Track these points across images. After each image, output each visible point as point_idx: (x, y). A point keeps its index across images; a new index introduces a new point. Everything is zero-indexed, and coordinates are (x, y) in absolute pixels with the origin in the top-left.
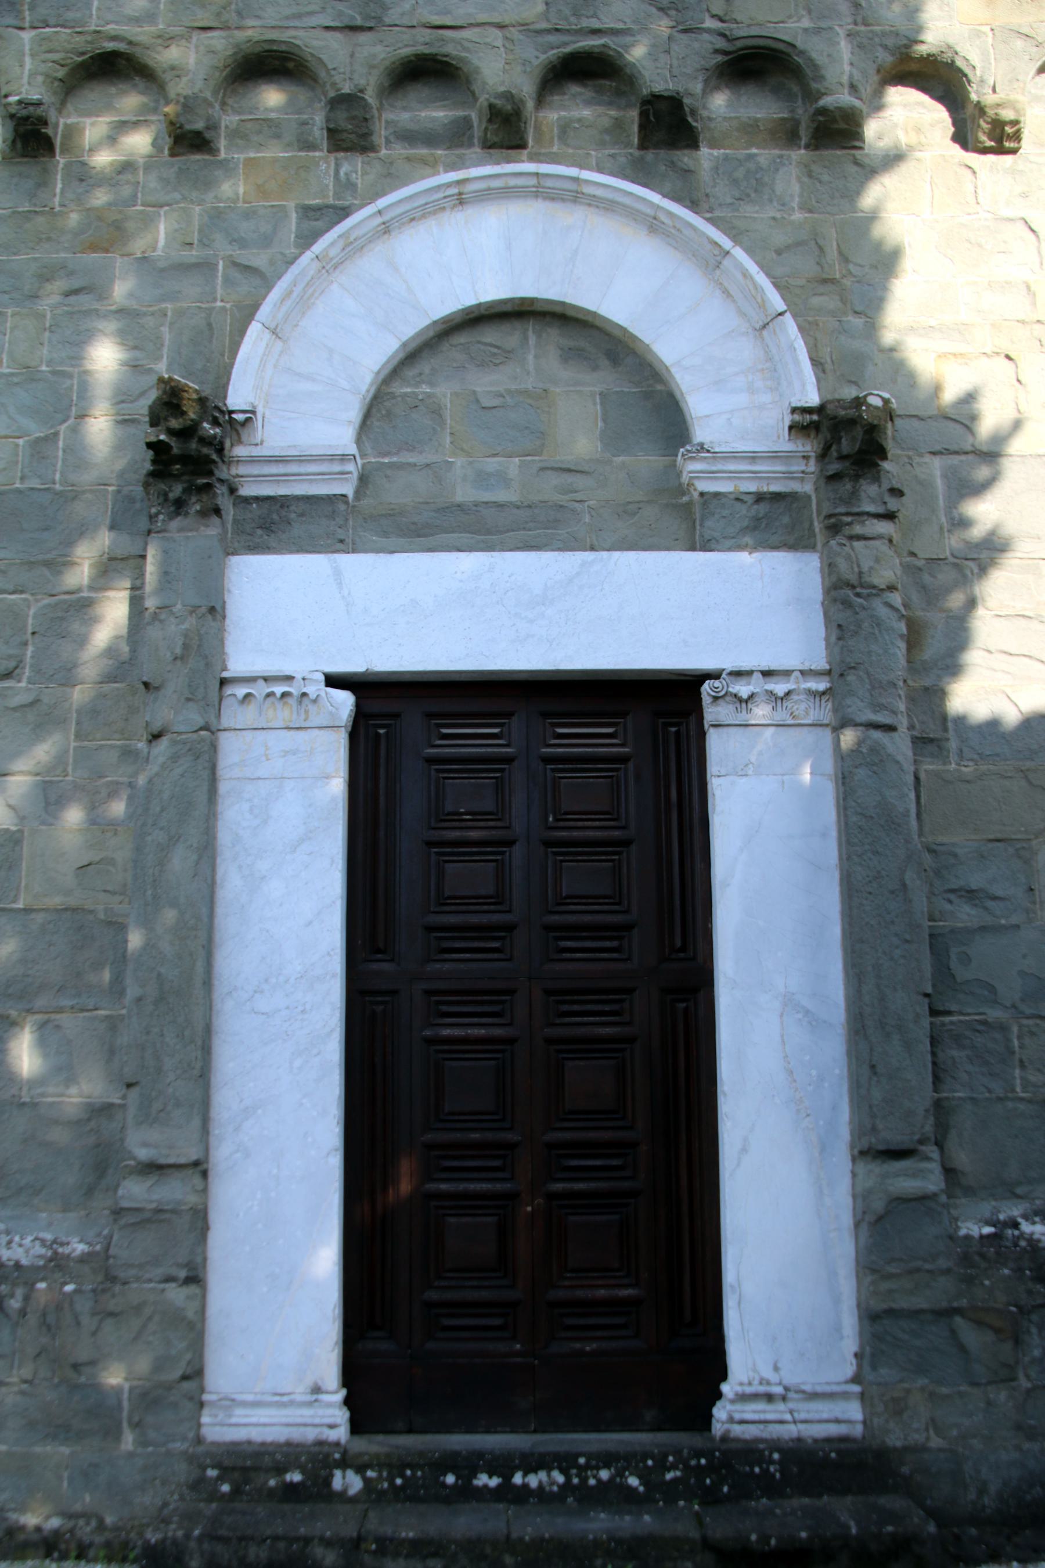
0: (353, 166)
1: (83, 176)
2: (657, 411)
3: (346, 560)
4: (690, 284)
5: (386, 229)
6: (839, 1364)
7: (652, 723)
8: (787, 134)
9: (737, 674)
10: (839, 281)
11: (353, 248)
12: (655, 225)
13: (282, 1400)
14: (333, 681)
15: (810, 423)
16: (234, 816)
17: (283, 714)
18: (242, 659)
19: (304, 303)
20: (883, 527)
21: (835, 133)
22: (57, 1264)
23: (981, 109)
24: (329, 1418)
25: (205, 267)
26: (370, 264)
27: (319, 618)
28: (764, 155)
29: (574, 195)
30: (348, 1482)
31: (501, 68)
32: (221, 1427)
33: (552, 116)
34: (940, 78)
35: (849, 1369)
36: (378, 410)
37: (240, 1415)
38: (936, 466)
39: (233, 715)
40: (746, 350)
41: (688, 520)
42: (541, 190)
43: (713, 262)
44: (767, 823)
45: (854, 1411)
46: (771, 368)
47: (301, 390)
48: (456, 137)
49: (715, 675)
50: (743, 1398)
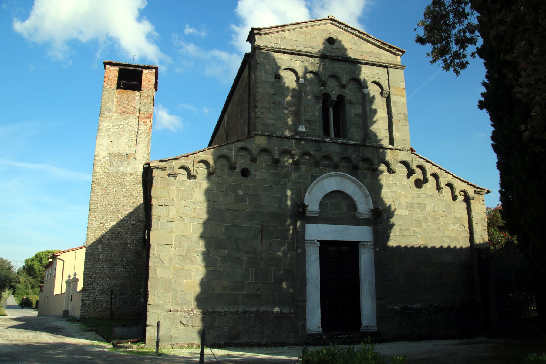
0: (317, 170)
1: (283, 167)
2: (353, 206)
3: (318, 225)
4: (358, 190)
5: (322, 180)
6: (374, 323)
7: (352, 248)
8: (368, 169)
9: (364, 242)
10: (375, 189)
11: (318, 182)
12: (354, 181)
13: (315, 329)
14: (318, 241)
15: (372, 211)
16: (307, 257)
17: (312, 245)
18: (307, 238)
19: (312, 189)
20: (380, 225)
21: (376, 172)
22: (290, 313)
23: (391, 169)
24: (320, 330)
25: (299, 182)
26: (320, 184)
27: (316, 232)
28: (366, 172)
29: (344, 176)
30: (324, 337)
31: (336, 158)
32: (309, 332)
33: (341, 164)
34: (387, 164)
35: (375, 324)
36: (322, 205)
37: (311, 330)
38: (385, 215)
39: (307, 245)
40: (364, 199)
41: (358, 222)
42: (341, 176)
43: (361, 187)
44: (366, 260)
45: (376, 328)
46: (367, 202)
47: (313, 201)
48: (329, 166)
49: (361, 242)
50: (365, 327)
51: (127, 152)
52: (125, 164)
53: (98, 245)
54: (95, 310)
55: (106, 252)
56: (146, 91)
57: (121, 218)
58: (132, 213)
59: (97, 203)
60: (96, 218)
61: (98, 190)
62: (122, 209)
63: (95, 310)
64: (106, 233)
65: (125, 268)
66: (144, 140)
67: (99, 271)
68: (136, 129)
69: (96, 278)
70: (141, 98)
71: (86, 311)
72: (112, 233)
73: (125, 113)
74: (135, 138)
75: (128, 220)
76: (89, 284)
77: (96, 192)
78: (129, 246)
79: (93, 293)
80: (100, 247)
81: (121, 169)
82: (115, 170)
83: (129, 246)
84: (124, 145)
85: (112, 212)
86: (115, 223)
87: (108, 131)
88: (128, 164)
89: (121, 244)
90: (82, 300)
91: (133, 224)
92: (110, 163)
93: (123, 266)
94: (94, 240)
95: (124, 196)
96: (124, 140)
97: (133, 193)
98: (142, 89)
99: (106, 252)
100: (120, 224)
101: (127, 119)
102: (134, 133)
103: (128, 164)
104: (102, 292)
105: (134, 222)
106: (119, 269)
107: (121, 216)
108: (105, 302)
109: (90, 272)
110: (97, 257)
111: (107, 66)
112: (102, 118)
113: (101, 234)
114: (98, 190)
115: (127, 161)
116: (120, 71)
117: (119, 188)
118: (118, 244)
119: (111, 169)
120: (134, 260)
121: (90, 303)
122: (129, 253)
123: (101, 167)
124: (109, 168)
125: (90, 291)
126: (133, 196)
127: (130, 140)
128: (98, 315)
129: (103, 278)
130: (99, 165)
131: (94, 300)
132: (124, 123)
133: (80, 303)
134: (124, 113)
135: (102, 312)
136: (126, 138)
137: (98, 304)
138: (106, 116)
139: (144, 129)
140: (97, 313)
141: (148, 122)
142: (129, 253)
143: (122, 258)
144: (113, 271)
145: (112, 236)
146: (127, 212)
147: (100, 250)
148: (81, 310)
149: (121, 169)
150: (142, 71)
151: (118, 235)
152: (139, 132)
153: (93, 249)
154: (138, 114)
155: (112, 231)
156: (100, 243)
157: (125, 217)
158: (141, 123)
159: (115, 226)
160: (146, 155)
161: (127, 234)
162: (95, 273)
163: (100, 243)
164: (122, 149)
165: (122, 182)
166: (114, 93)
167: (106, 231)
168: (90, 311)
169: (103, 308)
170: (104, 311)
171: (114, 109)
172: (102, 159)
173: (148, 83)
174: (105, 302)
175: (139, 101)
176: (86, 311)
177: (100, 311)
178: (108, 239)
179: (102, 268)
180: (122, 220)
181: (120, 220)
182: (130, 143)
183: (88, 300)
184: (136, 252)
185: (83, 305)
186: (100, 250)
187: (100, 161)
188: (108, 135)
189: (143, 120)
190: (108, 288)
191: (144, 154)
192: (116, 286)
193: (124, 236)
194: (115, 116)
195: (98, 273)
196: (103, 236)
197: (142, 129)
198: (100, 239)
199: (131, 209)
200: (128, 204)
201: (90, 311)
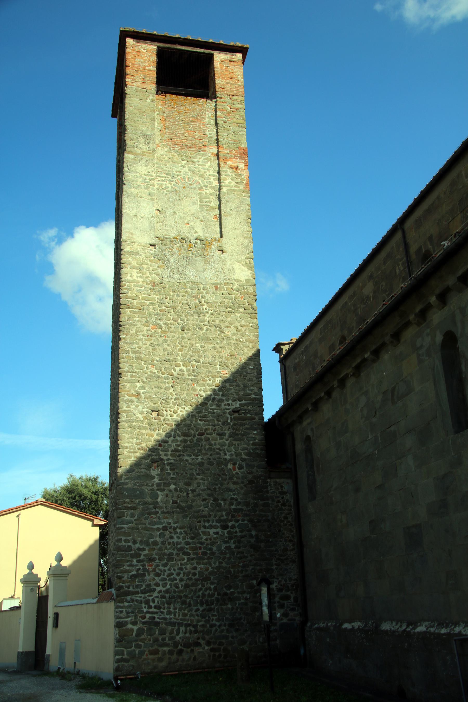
51: (200, 234)
52: (200, 262)
53: (149, 467)
54: (155, 652)
55: (173, 487)
56: (227, 98)
57: (204, 394)
58: (227, 381)
59: (138, 358)
60: (138, 395)
61: (139, 325)
62: (204, 373)
63: (155, 652)
64: (168, 435)
65: (225, 527)
66: (239, 207)
67: (158, 539)
68: (215, 183)
69: (151, 560)
70: (219, 113)
71: (132, 655)
72: (184, 435)
73: (185, 147)
74: (214, 203)
75: (221, 401)
76: (133, 577)
77: (133, 331)
78: (230, 466)
79: (147, 602)
80: (155, 472)
81: (191, 273)
82: (176, 276)
83: (230, 466)
84: (192, 219)
85: (177, 380)
86: (188, 409)
87: (148, 185)
88: (206, 262)
89: (211, 463)
90: (119, 625)
91: (235, 411)
92: (162, 260)
93: (219, 521)
94: (138, 454)
95: (205, 339)
96: (190, 207)
97: (226, 331)
98: (218, 94)
99: (173, 487)
100: (201, 408)
101: (190, 160)
102: (210, 191)
103: (206, 262)
104: (171, 598)
105: (237, 404)
106: (211, 531)
107: (204, 390)
108: (180, 624)
109: (135, 542)
110: (149, 500)
111: (129, 41)
112: (131, 156)
113: (156, 437)
114: (139, 325)
115: (203, 256)
116: (161, 53)
117: (192, 321)
118: (201, 464)
119: (166, 274)
120: (247, 504)
121: (140, 632)
122: (232, 486)
123: (140, 269)
124: (159, 271)
125: (137, 597)
126: (228, 338)
127: (203, 206)
128: (164, 664)
129: (170, 558)
130: (134, 263)
131: (153, 623)
132: (183, 169)
133: (111, 634)
134: (182, 147)
135: (174, 657)
136: (194, 203)
137: (163, 632)
138: (139, 151)
139: (233, 183)
140: (161, 660)
141: (242, 166)
142: (232, 486)
143: (215, 500)
144: (196, 536)
145: (185, 441)
146: (218, 381)
147: (156, 480)
148: (116, 653)
149: (191, 273)
150: (212, 55)
151: (199, 440)
152: (224, 190)
153: (138, 477)
154: (215, 150)
155: (184, 427)
156: (153, 461)
157: (214, 390)
158: (224, 168)
159: (190, 416)
160: (246, 241)
161: (221, 435)
162: (147, 544)
163: (153, 461)
164: (185, 228)
165: (196, 306)
166: (153, 101)
167: (168, 428)
168: (142, 653)
169: (176, 644)
170: (180, 652)
171: (157, 137)
172: (140, 249)
173: (230, 81)
174: (180, 624)
175: (213, 122)
176: (132, 655)
177: (171, 653)
178: (175, 451)
179: (165, 529)
180: (207, 399)
181: (201, 400)
182: (205, 213)
183: (134, 623)
184: (250, 482)
185: (122, 639)
186: (156, 480)
187: (137, 253)
188: (150, 194)
189: (229, 163)
190: (186, 586)
191: (241, 239)
192: (207, 579)
193: (216, 442)
194: (161, 151)
195: (155, 543)
196: (161, 443)
197: (228, 181)
198: (152, 450)
199: (226, 373)
200: (217, 360)
201: (142, 653)
